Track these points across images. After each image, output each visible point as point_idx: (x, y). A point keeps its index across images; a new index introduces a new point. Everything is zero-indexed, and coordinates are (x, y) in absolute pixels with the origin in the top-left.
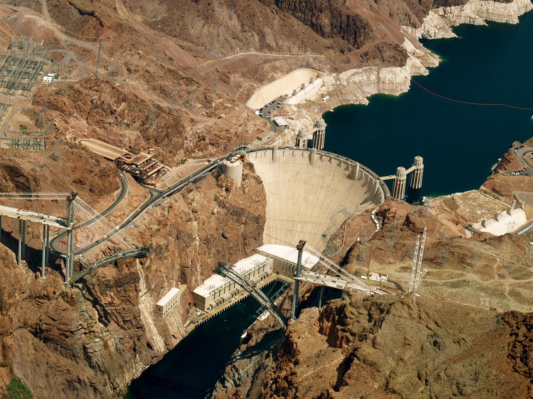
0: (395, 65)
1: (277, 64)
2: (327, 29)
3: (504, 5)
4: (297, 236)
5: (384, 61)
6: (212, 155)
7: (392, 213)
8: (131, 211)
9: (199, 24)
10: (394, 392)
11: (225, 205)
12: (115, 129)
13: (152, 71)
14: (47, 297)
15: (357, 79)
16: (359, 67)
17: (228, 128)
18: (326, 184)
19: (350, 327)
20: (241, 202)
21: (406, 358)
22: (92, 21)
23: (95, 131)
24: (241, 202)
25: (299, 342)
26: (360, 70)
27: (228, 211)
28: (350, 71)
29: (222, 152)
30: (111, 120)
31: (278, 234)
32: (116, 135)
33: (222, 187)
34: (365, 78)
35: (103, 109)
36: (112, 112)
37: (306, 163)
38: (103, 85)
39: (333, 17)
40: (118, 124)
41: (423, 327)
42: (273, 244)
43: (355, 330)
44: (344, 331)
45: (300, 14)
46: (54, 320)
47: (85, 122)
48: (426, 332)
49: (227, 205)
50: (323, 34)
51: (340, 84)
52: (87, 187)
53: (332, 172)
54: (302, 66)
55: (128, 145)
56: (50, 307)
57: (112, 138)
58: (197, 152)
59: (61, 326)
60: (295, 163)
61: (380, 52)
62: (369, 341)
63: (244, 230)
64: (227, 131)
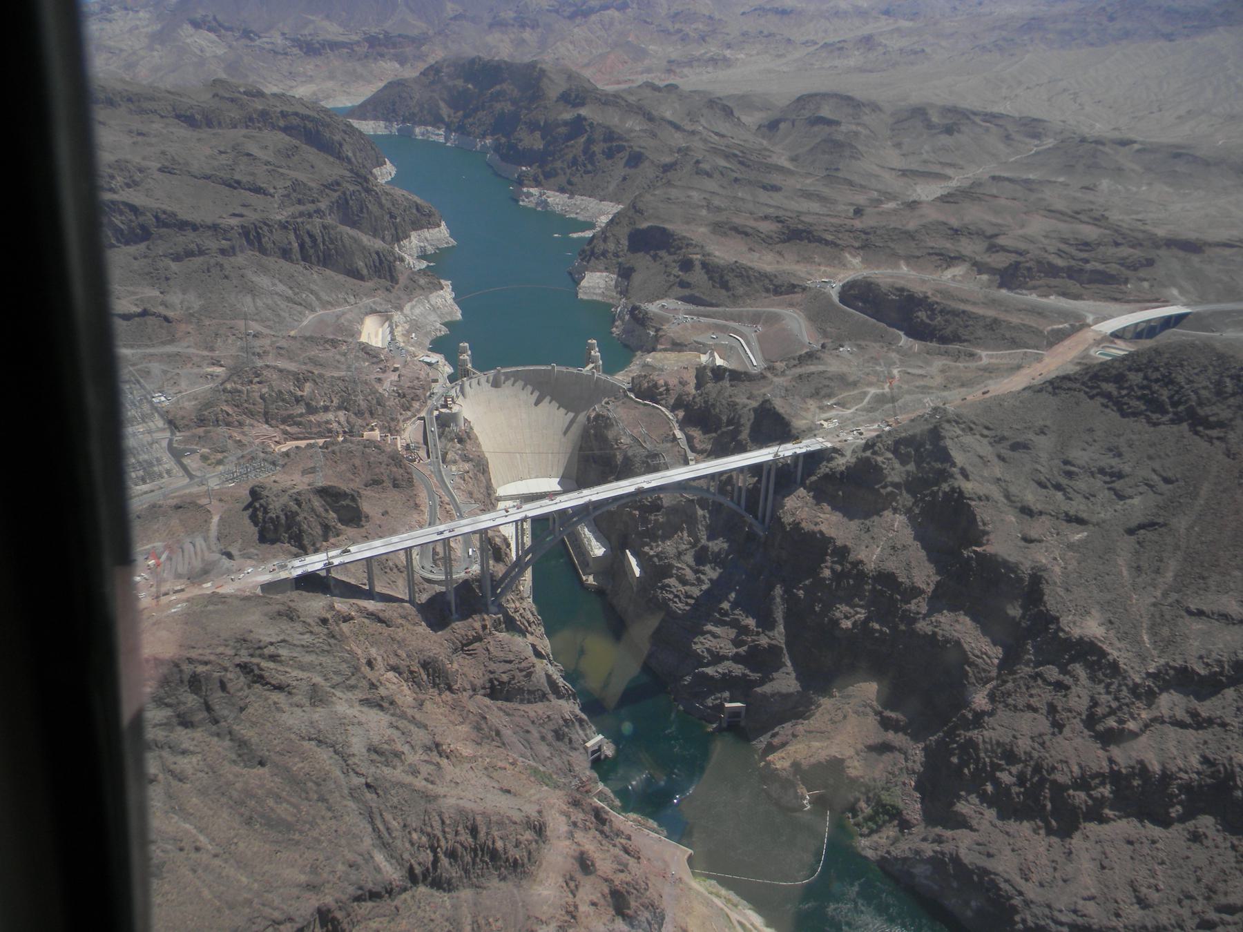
1: (348, 316)
2: (365, 272)
6: (419, 411)
9: (248, 299)
10: (1041, 513)
12: (312, 418)
13: (285, 345)
14: (478, 639)
16: (410, 300)
19: (889, 479)
21: (999, 476)
22: (150, 320)
23: (285, 432)
25: (823, 528)
30: (301, 409)
32: (319, 424)
35: (283, 400)
36: (298, 400)
38: (265, 373)
40: (312, 410)
41: (978, 437)
43: (897, 479)
44: (885, 487)
46: (510, 662)
47: (266, 426)
48: (985, 441)
50: (362, 278)
52: (388, 484)
54: (366, 314)
55: (340, 430)
56: (491, 649)
57: (315, 430)
59: (524, 665)
62: (959, 477)
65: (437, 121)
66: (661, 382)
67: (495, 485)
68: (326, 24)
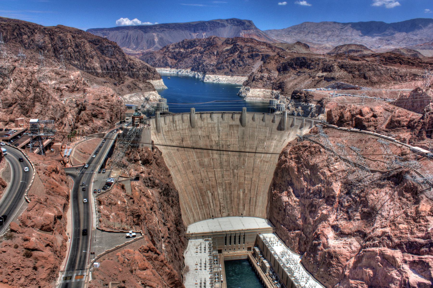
0: (150, 91)
3: (158, 81)
4: (212, 204)
5: (141, 90)
7: (368, 113)
8: (65, 207)
11: (154, 183)
15: (134, 99)
17: (105, 95)
18: (214, 143)
20: (162, 177)
24: (162, 177)
26: (133, 94)
27: (162, 189)
28: (127, 95)
29: (110, 124)
31: (193, 210)
33: (136, 161)
34: (138, 98)
37: (187, 127)
39: (101, 62)
42: (193, 223)
45: (76, 62)
49: (157, 181)
50: (97, 75)
51: (128, 102)
53: (216, 128)
58: (81, 126)
60: (177, 130)
61: (136, 85)
63: (174, 213)
64: (105, 97)
65: (166, 65)
66: (366, 109)
67: (185, 222)
68: (128, 49)
